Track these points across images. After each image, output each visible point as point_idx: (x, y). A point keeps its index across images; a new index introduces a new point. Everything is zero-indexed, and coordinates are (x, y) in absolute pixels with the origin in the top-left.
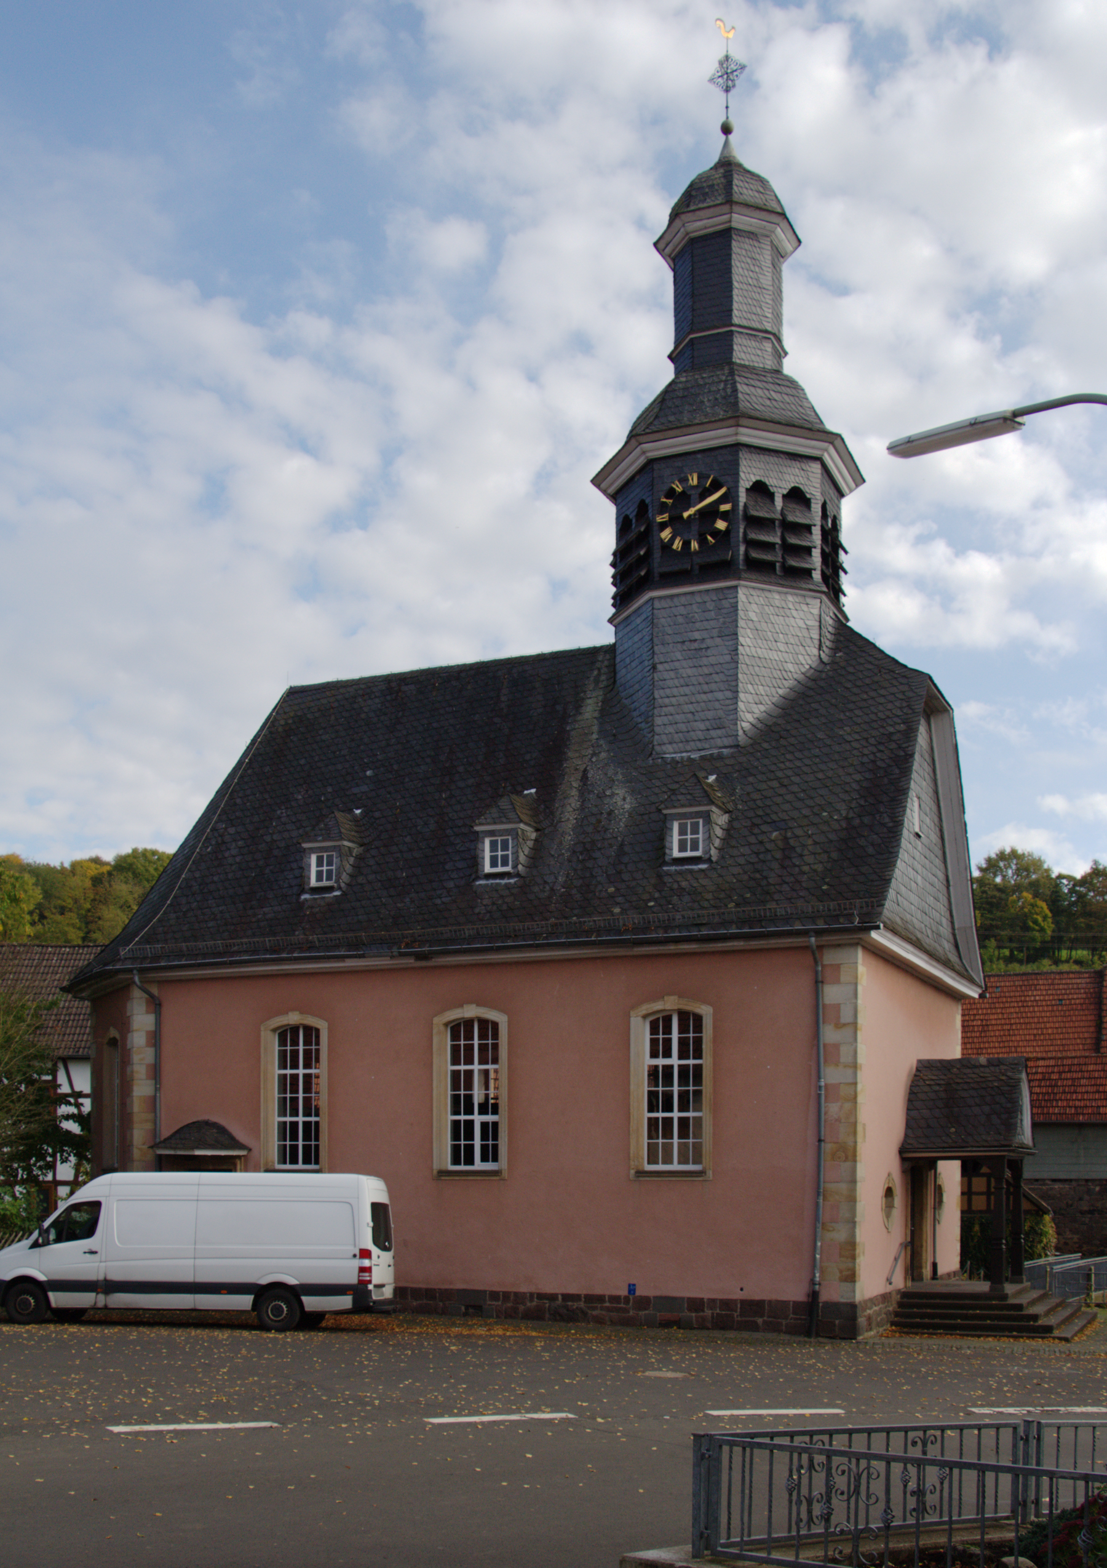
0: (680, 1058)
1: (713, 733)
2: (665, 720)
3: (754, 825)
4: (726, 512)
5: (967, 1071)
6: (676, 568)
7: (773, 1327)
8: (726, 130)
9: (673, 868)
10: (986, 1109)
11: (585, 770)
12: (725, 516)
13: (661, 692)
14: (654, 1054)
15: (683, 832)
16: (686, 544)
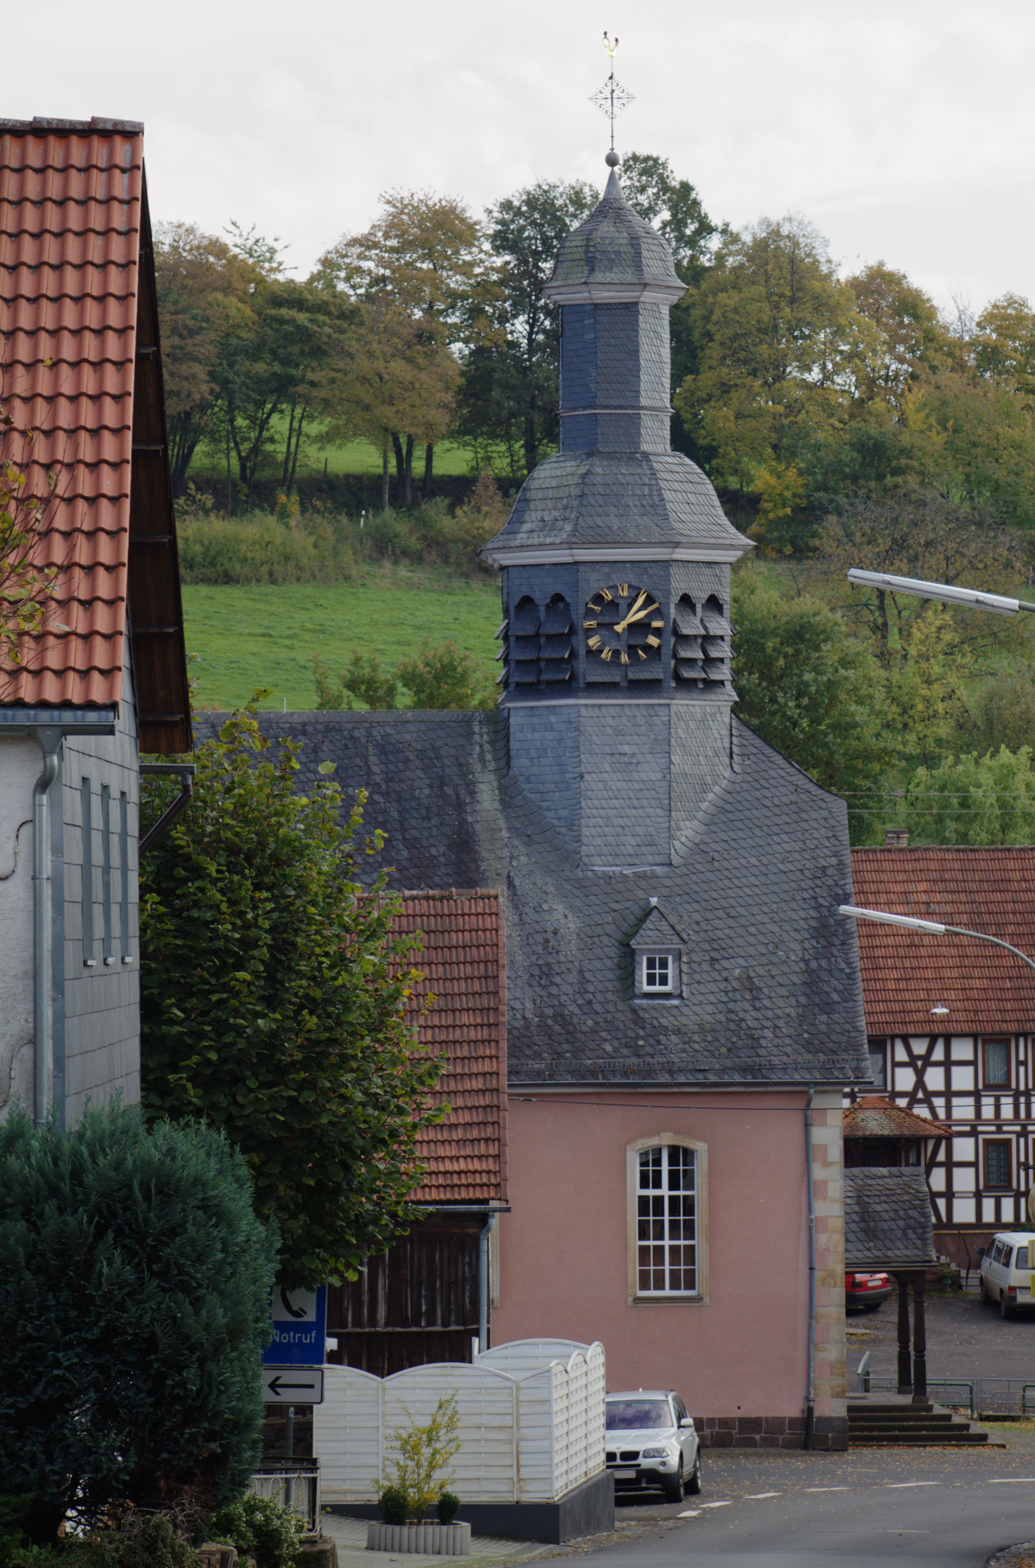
0: (671, 1189)
1: (644, 849)
2: (593, 831)
3: (713, 959)
5: (870, 1182)
7: (770, 1443)
9: (644, 1001)
10: (902, 1223)
11: (509, 877)
12: (658, 632)
13: (589, 802)
14: (644, 1185)
15: (651, 964)
16: (616, 653)
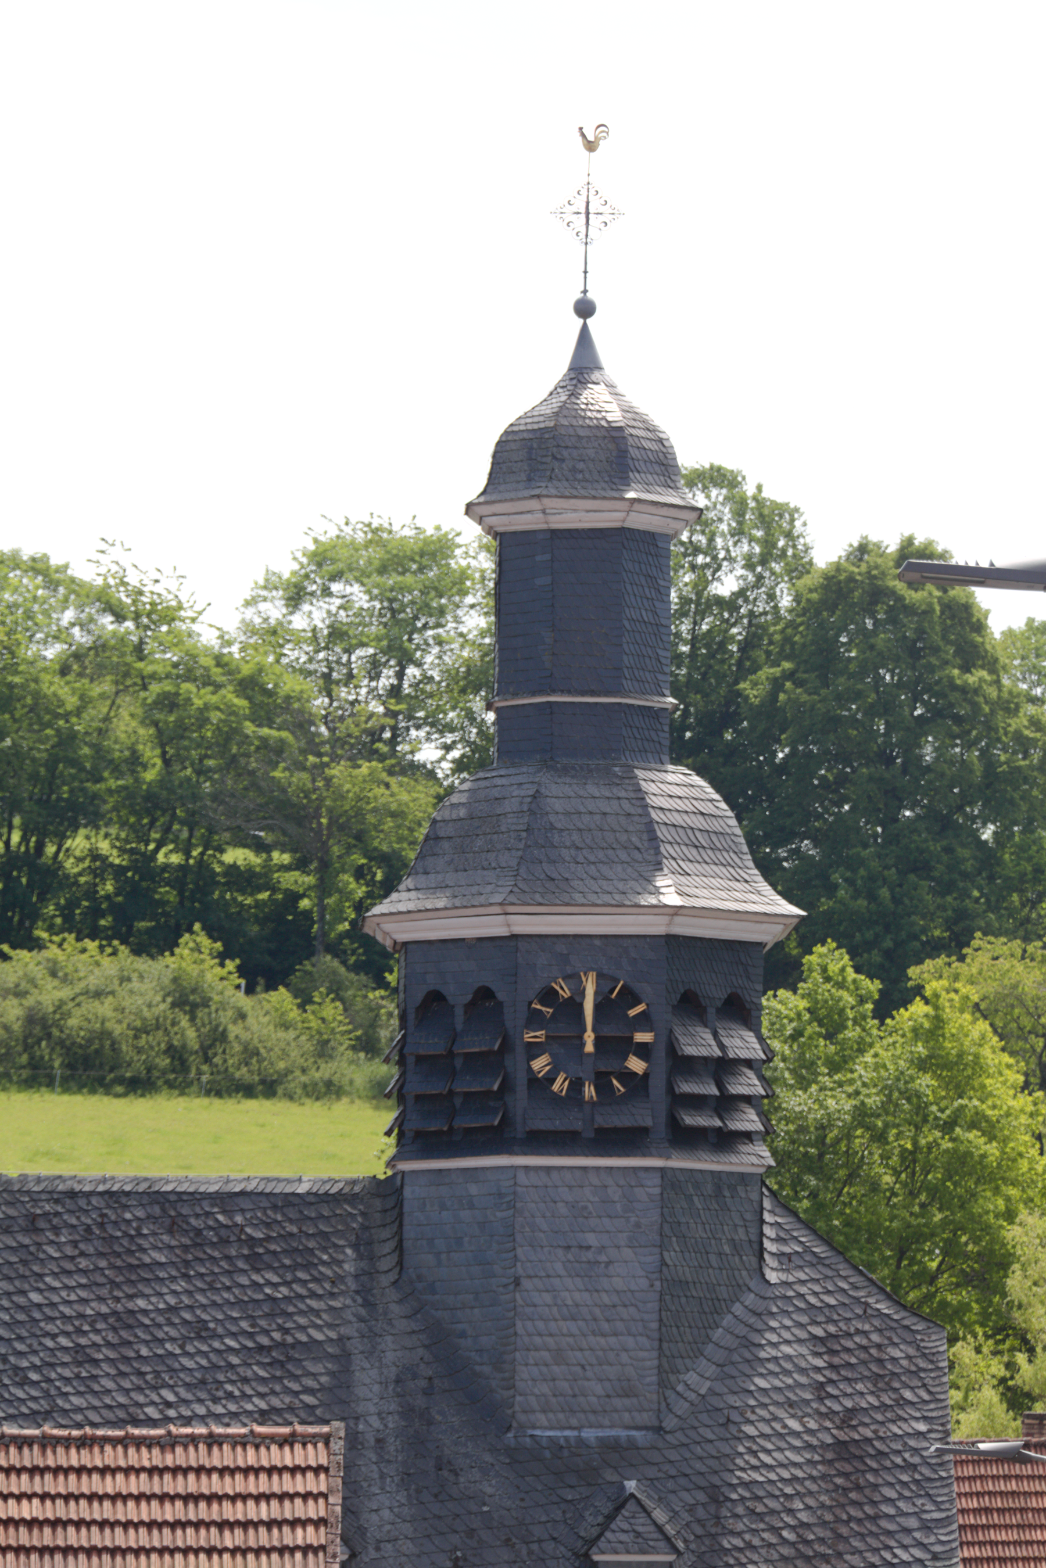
1: (618, 1402)
4: (645, 1045)
6: (558, 1125)
8: (585, 309)
12: (643, 1051)
16: (576, 1086)
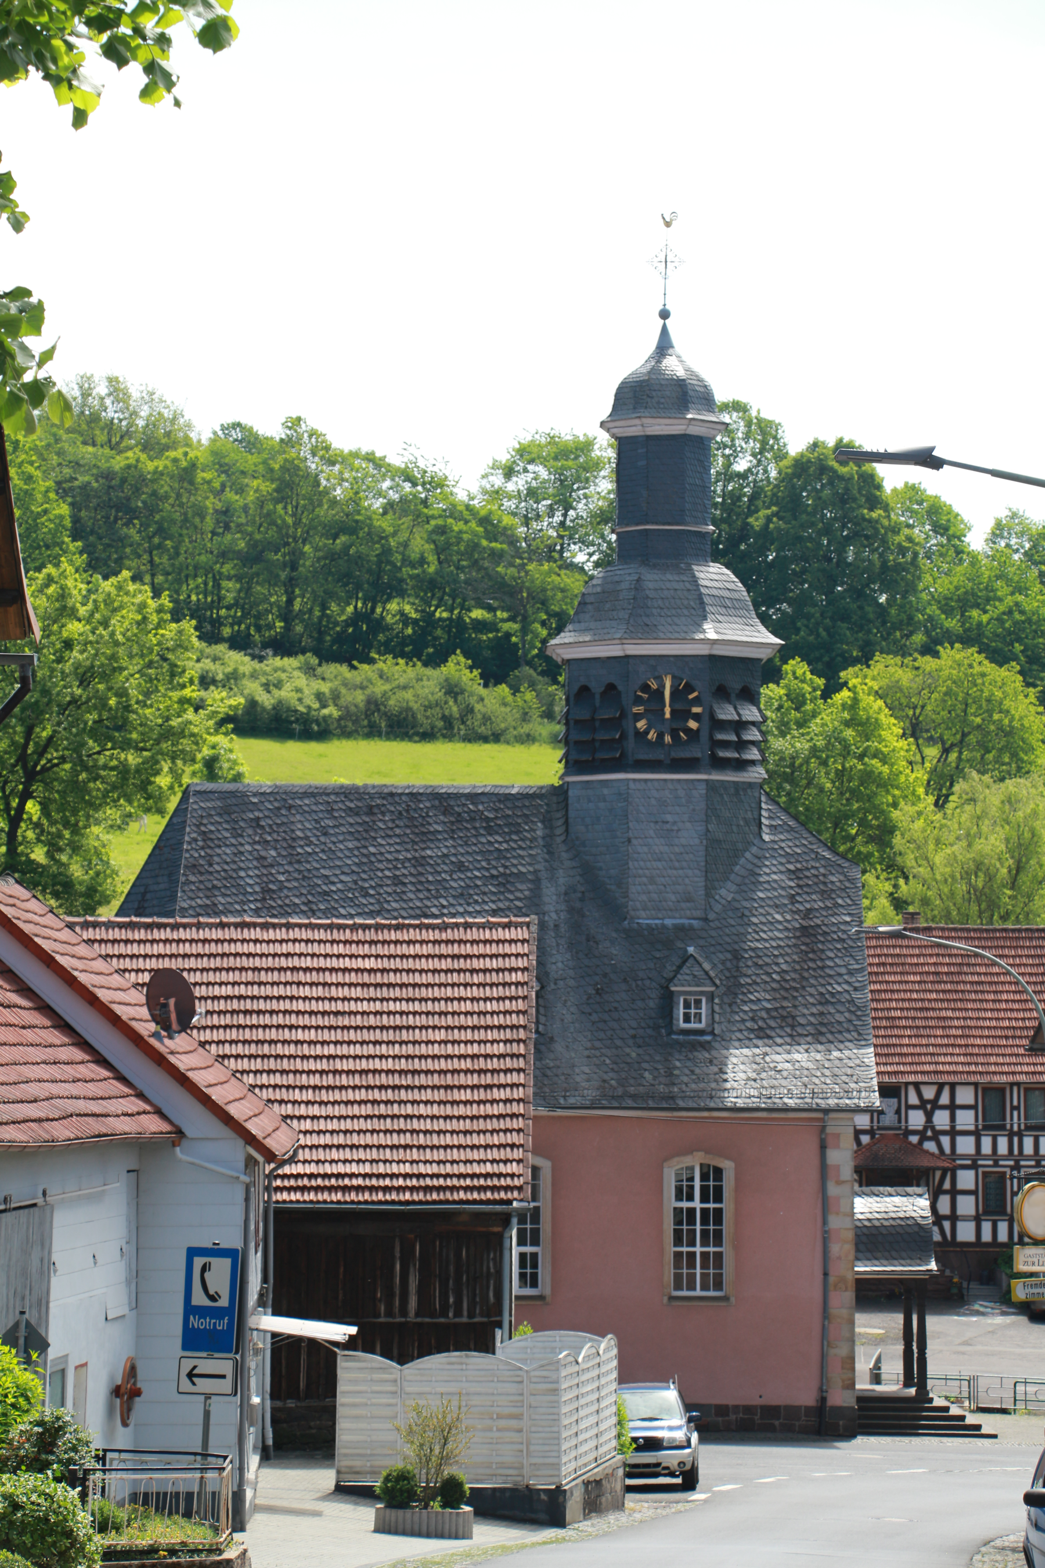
0: (702, 1201)
1: (683, 905)
4: (697, 714)
6: (650, 756)
8: (664, 315)
12: (697, 717)
15: (687, 1005)
16: (660, 736)
